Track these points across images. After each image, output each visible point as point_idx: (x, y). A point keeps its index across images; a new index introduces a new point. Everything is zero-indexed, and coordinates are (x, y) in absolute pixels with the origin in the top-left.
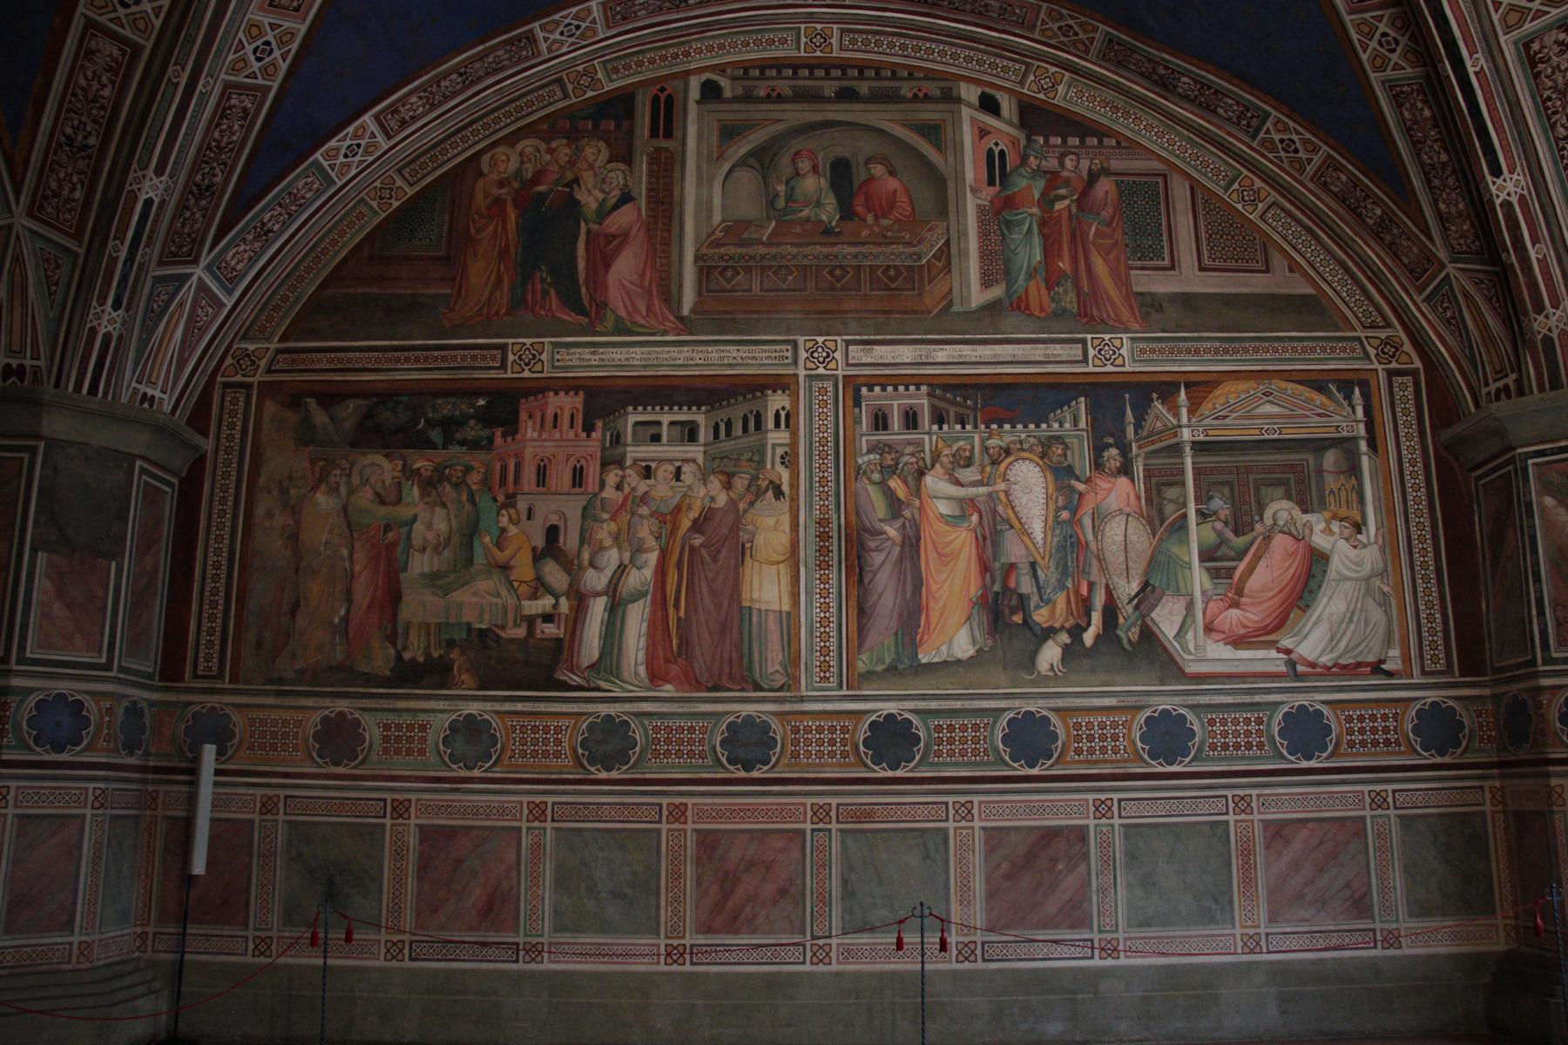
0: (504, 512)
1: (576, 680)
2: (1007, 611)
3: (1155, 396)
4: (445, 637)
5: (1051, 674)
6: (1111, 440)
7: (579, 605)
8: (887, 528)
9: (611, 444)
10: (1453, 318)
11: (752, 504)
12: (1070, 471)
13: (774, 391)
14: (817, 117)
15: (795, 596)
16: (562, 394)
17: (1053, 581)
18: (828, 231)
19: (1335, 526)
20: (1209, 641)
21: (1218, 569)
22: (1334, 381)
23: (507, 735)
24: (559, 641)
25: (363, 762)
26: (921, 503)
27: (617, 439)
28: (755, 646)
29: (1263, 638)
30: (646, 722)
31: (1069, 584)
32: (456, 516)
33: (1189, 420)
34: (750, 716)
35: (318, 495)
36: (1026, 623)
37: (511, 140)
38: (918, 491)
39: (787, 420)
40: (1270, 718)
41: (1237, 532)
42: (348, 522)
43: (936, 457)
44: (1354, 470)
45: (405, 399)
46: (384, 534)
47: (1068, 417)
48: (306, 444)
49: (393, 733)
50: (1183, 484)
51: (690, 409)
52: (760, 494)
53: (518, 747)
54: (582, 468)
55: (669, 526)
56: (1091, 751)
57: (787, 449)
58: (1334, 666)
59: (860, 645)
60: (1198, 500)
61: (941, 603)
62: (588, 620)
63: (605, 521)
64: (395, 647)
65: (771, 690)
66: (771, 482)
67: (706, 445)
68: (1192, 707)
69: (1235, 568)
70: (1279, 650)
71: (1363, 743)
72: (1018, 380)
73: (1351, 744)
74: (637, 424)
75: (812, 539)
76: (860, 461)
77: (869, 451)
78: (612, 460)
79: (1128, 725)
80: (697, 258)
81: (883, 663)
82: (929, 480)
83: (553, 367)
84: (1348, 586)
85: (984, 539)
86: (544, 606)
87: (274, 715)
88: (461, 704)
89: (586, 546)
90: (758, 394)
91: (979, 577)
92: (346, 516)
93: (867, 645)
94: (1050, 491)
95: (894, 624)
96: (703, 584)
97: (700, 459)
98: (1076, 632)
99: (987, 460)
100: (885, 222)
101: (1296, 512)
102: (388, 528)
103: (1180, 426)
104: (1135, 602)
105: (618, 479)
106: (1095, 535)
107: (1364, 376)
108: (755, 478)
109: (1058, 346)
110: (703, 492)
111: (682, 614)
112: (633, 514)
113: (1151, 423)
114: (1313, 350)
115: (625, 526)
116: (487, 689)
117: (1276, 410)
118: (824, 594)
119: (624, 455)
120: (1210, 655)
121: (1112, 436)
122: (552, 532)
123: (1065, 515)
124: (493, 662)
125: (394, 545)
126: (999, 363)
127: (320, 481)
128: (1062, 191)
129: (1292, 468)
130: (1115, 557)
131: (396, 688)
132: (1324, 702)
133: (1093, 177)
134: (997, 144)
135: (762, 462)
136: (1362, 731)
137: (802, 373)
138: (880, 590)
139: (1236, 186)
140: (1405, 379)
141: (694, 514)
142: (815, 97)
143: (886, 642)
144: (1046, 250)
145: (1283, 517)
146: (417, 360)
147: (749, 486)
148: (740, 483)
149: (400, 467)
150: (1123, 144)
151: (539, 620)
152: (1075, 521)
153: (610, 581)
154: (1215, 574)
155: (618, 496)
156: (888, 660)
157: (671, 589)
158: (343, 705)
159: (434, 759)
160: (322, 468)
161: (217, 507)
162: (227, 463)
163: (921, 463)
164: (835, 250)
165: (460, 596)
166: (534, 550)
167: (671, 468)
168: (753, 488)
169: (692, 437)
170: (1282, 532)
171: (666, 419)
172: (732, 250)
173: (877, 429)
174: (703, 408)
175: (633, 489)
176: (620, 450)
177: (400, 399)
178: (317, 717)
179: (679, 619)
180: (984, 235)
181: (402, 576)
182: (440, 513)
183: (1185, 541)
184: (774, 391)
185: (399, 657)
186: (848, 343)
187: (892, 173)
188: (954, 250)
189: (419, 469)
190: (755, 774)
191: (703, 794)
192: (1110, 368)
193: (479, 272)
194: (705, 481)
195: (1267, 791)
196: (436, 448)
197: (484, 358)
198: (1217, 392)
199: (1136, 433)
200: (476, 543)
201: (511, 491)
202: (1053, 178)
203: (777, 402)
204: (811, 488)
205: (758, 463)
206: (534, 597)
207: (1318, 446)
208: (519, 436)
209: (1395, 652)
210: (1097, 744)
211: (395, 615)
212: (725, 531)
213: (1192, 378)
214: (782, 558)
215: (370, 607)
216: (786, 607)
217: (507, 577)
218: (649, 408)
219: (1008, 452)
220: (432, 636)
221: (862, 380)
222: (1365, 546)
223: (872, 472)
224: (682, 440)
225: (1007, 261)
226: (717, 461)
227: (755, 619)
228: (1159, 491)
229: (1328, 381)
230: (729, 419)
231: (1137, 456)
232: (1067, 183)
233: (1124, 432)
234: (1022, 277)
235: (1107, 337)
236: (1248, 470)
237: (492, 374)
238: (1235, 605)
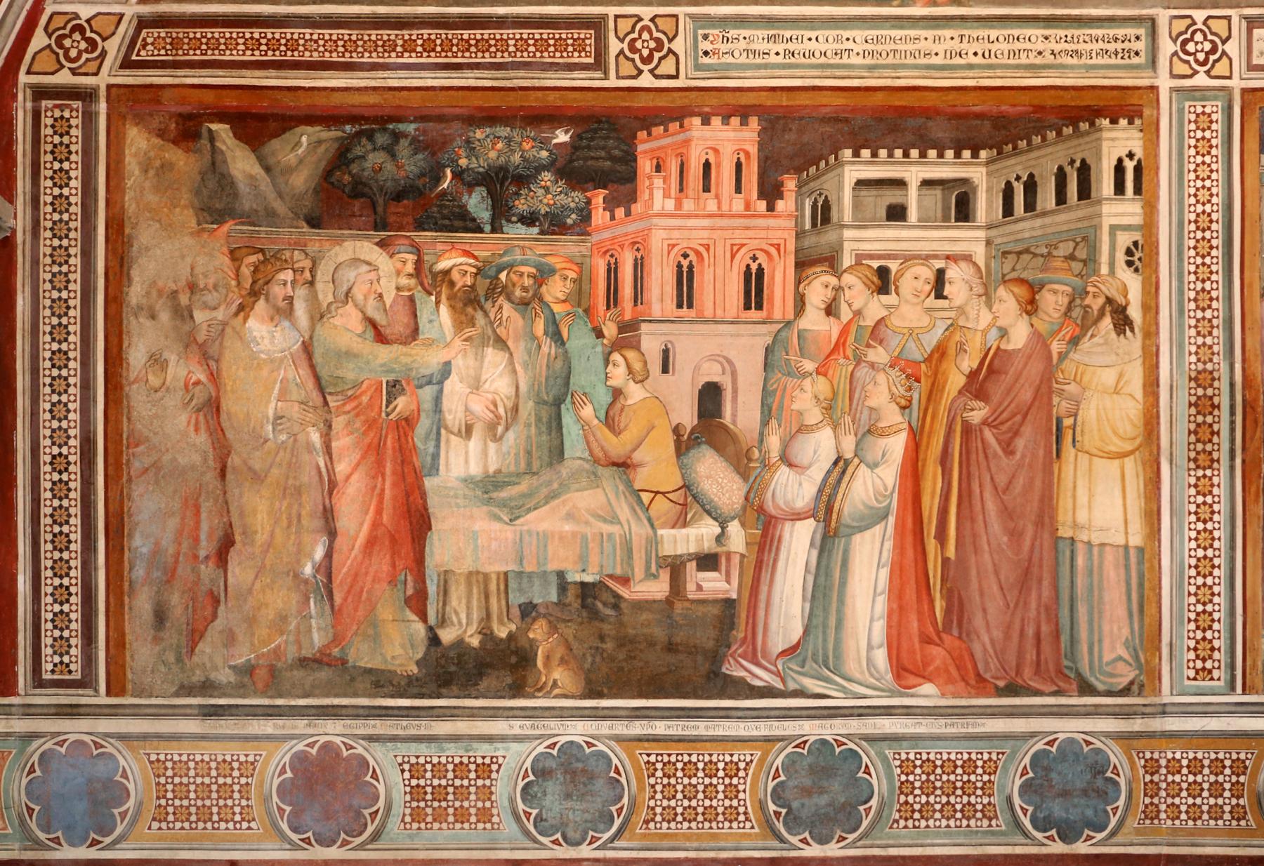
0: (616, 357)
4: (516, 599)
7: (764, 535)
9: (814, 225)
11: (1074, 341)
13: (1114, 121)
15: (1152, 517)
16: (716, 121)
23: (640, 780)
24: (729, 604)
25: (376, 836)
27: (824, 215)
28: (1082, 610)
30: (889, 753)
32: (525, 366)
34: (1071, 741)
35: (252, 323)
42: (317, 379)
45: (411, 128)
46: (389, 403)
48: (219, 216)
49: (429, 780)
51: (958, 155)
52: (1087, 323)
53: (660, 802)
54: (760, 270)
55: (925, 383)
57: (1137, 236)
62: (781, 564)
63: (805, 375)
64: (424, 617)
65: (1109, 693)
66: (1109, 300)
67: (990, 227)
74: (860, 183)
75: (1182, 410)
83: (698, 67)
86: (700, 539)
87: (202, 752)
88: (553, 725)
89: (774, 423)
90: (1084, 126)
92: (312, 367)
96: (988, 495)
97: (979, 253)
102: (395, 388)
105: (830, 294)
110: (985, 318)
111: (951, 552)
112: (859, 361)
115: (844, 386)
116: (600, 695)
118: (1204, 515)
122: (710, 397)
124: (609, 646)
125: (408, 423)
127: (255, 294)
131: (431, 697)
135: (1091, 262)
141: (969, 363)
146: (429, 47)
147: (1069, 308)
148: (1052, 302)
149: (410, 268)
151: (691, 566)
153: (820, 491)
155: (831, 328)
157: (930, 504)
158: (332, 731)
159: (509, 827)
160: (256, 270)
161: (47, 346)
162: (60, 256)
165: (541, 521)
166: (677, 430)
167: (927, 273)
168: (1078, 312)
169: (963, 210)
171: (914, 174)
174: (983, 154)
175: (858, 313)
176: (830, 236)
177: (402, 127)
178: (283, 755)
179: (946, 561)
181: (429, 483)
182: (491, 353)
184: (1114, 121)
185: (434, 640)
189: (447, 272)
194: (987, 296)
196: (481, 231)
197: (560, 45)
200: (568, 419)
201: (628, 316)
204: (1181, 311)
205: (1085, 262)
206: (682, 521)
208: (637, 208)
211: (420, 560)
212: (1027, 395)
214: (1128, 447)
215: (371, 543)
217: (629, 484)
218: (883, 153)
220: (494, 601)
224: (946, 218)
226: (1012, 257)
227: (1080, 561)
230: (1031, 176)
237: (580, 79)
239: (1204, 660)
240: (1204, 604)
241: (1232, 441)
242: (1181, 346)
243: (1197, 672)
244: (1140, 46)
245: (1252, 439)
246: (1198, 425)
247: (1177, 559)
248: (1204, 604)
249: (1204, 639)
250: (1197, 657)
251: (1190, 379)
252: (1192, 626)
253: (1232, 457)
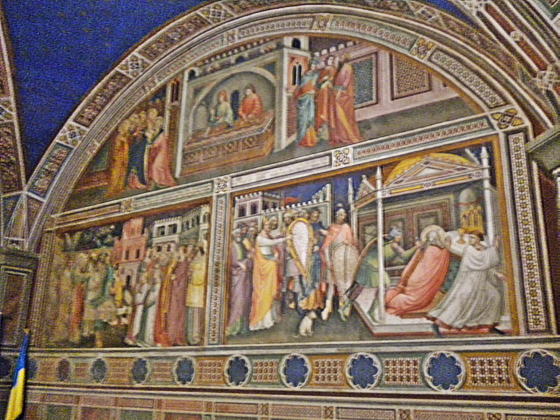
1: (130, 342)
3: (364, 176)
6: (340, 205)
11: (193, 258)
12: (320, 225)
14: (227, 75)
17: (310, 285)
18: (229, 126)
19: (466, 238)
20: (387, 314)
21: (393, 271)
27: (151, 237)
29: (419, 311)
31: (317, 285)
33: (382, 186)
37: (127, 117)
38: (253, 245)
39: (208, 218)
40: (422, 361)
41: (406, 248)
43: (263, 225)
44: (480, 200)
47: (321, 196)
50: (376, 224)
56: (324, 378)
58: (465, 327)
60: (384, 233)
68: (376, 354)
69: (403, 270)
70: (428, 318)
71: (483, 380)
72: (300, 181)
73: (475, 380)
78: (149, 245)
79: (342, 364)
80: (184, 150)
82: (259, 238)
84: (473, 275)
98: (319, 312)
99: (284, 225)
100: (250, 116)
101: (441, 231)
103: (376, 191)
104: (348, 293)
106: (330, 257)
107: (489, 139)
108: (195, 246)
113: (362, 191)
114: (456, 130)
119: (152, 243)
120: (387, 322)
121: (341, 202)
123: (316, 248)
126: (291, 174)
128: (326, 78)
129: (440, 205)
130: (339, 268)
132: (456, 352)
133: (341, 65)
134: (297, 63)
136: (483, 372)
137: (214, 195)
139: (415, 46)
140: (517, 135)
141: (173, 265)
142: (229, 65)
144: (316, 111)
145: (433, 235)
148: (190, 249)
150: (357, 42)
152: (321, 251)
154: (391, 274)
156: (238, 328)
164: (230, 135)
167: (166, 246)
169: (174, 231)
170: (432, 245)
172: (195, 144)
180: (289, 111)
183: (376, 256)
186: (232, 177)
187: (254, 92)
188: (276, 121)
190: (186, 386)
191: (169, 395)
192: (343, 166)
193: (116, 173)
194: (177, 250)
195: (420, 408)
198: (397, 168)
199: (354, 199)
202: (322, 72)
203: (205, 209)
207: (457, 189)
209: (506, 318)
210: (326, 374)
213: (384, 163)
214: (200, 283)
216: (201, 306)
219: (293, 219)
221: (236, 194)
222: (486, 248)
225: (298, 121)
228: (364, 230)
229: (465, 148)
232: (328, 73)
233: (347, 198)
234: (305, 127)
236: (413, 210)
238: (403, 291)
244: (210, 187)
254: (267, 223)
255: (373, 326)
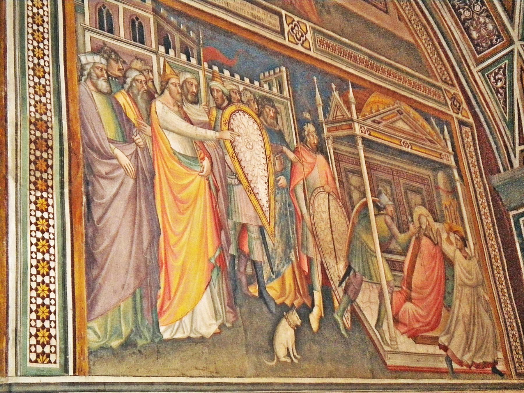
2: (244, 279)
5: (289, 361)
8: (117, 152)
10: (502, 88)
19: (452, 237)
22: (435, 117)
26: (153, 130)
33: (358, 118)
36: (262, 294)
59: (91, 307)
61: (181, 259)
76: (83, 60)
77: (96, 51)
81: (120, 335)
82: (158, 105)
85: (217, 190)
91: (216, 237)
93: (99, 309)
94: (268, 153)
95: (131, 282)
99: (212, 104)
104: (344, 285)
109: (261, 11)
117: (406, 128)
123: (283, 181)
138: (113, 231)
143: (122, 305)
152: (291, 190)
156: (125, 330)
163: (150, 84)
173: (101, 28)
183: (368, 229)
192: (299, 48)
199: (325, 117)
223: (98, 78)
231: (328, 138)
235: (296, 19)
239: (43, 346)
240: (43, 298)
241: (62, 175)
242: (24, 99)
243: (38, 356)
245: (76, 175)
246: (37, 158)
247: (21, 259)
248: (43, 298)
249: (43, 327)
250: (38, 342)
251: (31, 123)
252: (34, 316)
253: (62, 187)
254: (173, 80)
255: (385, 351)
